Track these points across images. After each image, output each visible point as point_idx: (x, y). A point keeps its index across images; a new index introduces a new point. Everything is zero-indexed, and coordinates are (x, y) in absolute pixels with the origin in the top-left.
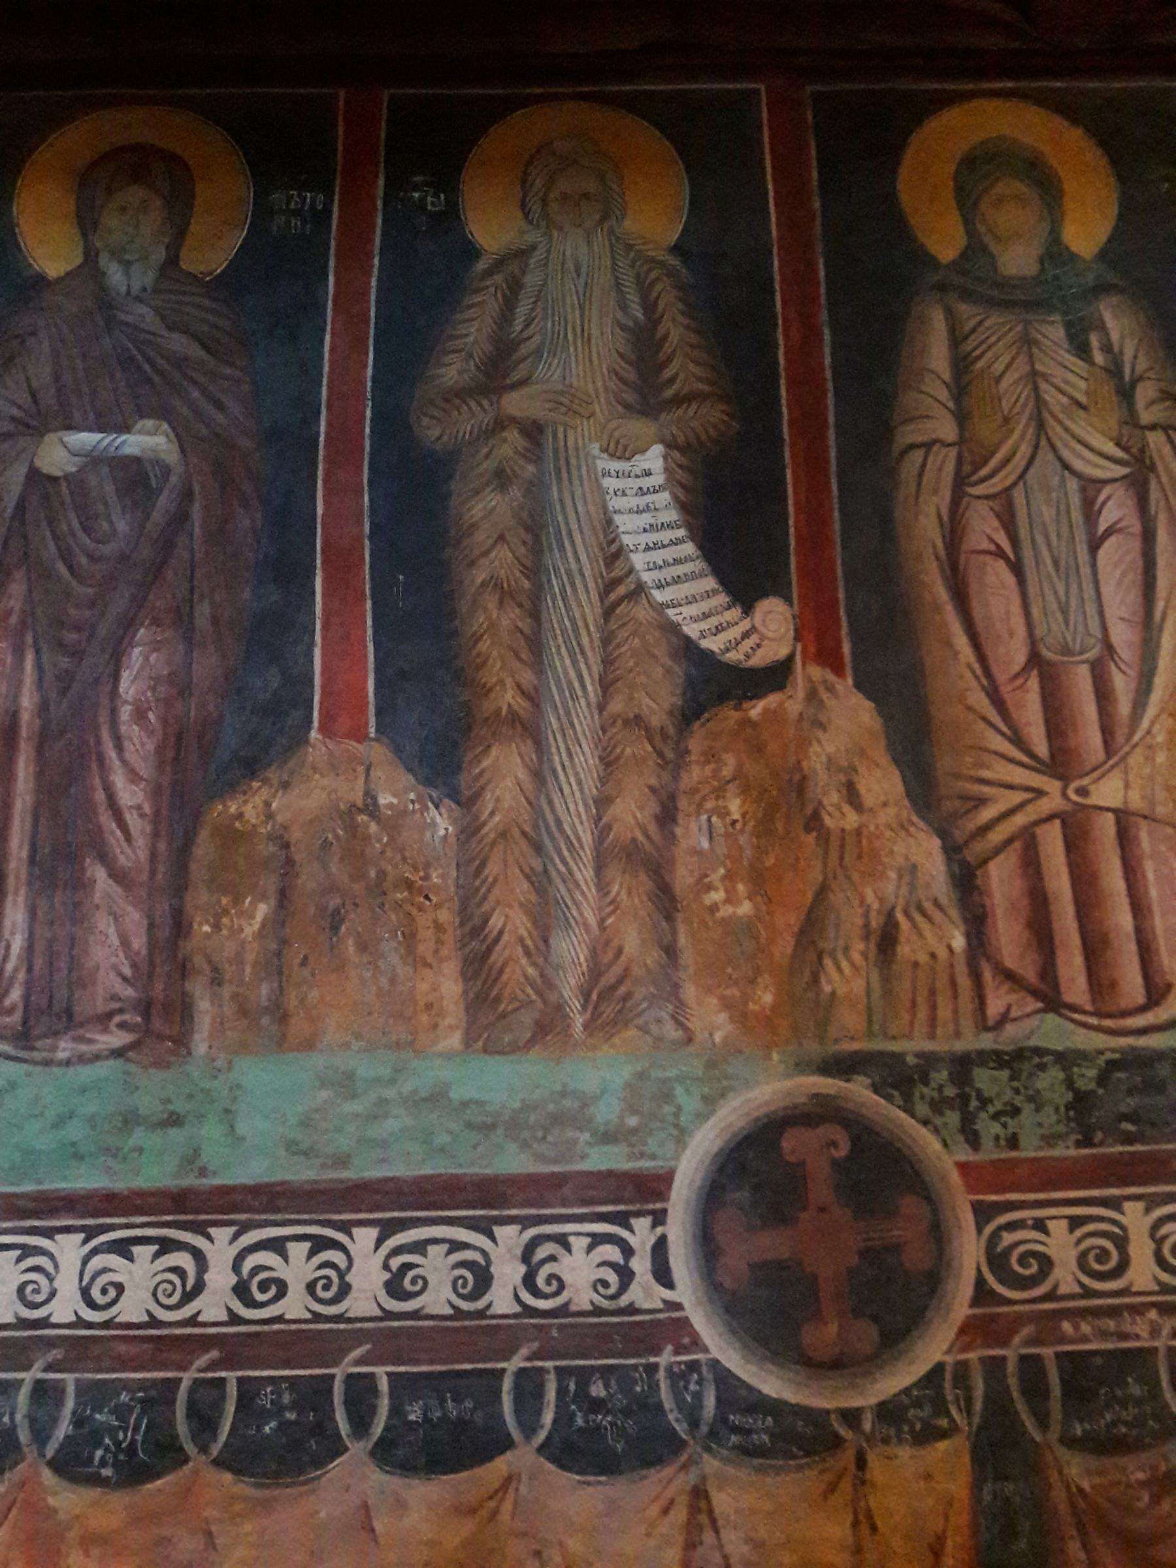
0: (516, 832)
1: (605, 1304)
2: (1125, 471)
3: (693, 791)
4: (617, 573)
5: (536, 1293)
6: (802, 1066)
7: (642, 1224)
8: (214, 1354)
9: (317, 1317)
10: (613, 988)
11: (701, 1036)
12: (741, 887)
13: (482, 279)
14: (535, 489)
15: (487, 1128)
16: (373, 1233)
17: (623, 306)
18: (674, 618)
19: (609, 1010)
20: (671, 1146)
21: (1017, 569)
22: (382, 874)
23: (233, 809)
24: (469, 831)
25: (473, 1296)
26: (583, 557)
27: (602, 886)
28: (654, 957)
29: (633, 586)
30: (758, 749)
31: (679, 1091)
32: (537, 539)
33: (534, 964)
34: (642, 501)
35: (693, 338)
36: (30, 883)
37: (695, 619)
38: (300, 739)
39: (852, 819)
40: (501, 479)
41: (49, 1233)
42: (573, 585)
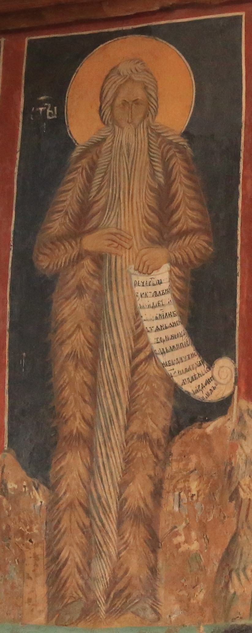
0: (77, 503)
3: (172, 478)
4: (139, 346)
10: (122, 591)
12: (193, 534)
13: (76, 162)
17: (153, 174)
18: (169, 372)
19: (119, 604)
22: (8, 526)
27: (120, 534)
28: (145, 573)
29: (148, 353)
30: (209, 451)
33: (83, 578)
34: (155, 300)
35: (191, 194)
40: (80, 290)
42: (115, 354)
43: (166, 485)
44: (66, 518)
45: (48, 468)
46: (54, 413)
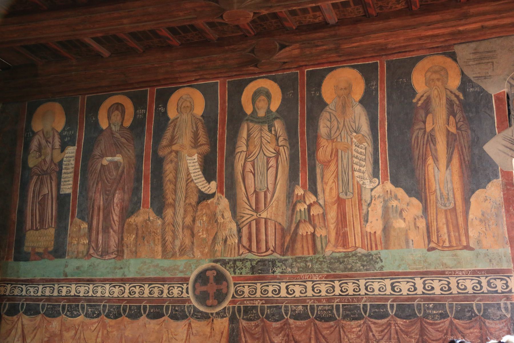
1: (179, 296)
2: (274, 155)
3: (198, 216)
4: (189, 178)
5: (169, 294)
6: (211, 261)
7: (185, 285)
8: (126, 302)
9: (140, 297)
10: (184, 249)
11: (196, 256)
12: (204, 232)
13: (170, 124)
14: (177, 163)
15: (164, 270)
16: (147, 285)
17: (193, 128)
19: (183, 253)
20: (190, 274)
21: (254, 175)
22: (150, 230)
23: (130, 220)
24: (163, 223)
25: (161, 295)
26: (184, 175)
27: (183, 232)
28: (190, 244)
30: (209, 208)
31: (192, 265)
32: (176, 172)
34: (193, 164)
35: (204, 133)
36: (102, 232)
37: (200, 185)
38: (139, 208)
39: (222, 220)
40: (171, 161)
41: (105, 284)
43: (196, 218)
44: (167, 228)
45: (162, 213)
46: (164, 197)
